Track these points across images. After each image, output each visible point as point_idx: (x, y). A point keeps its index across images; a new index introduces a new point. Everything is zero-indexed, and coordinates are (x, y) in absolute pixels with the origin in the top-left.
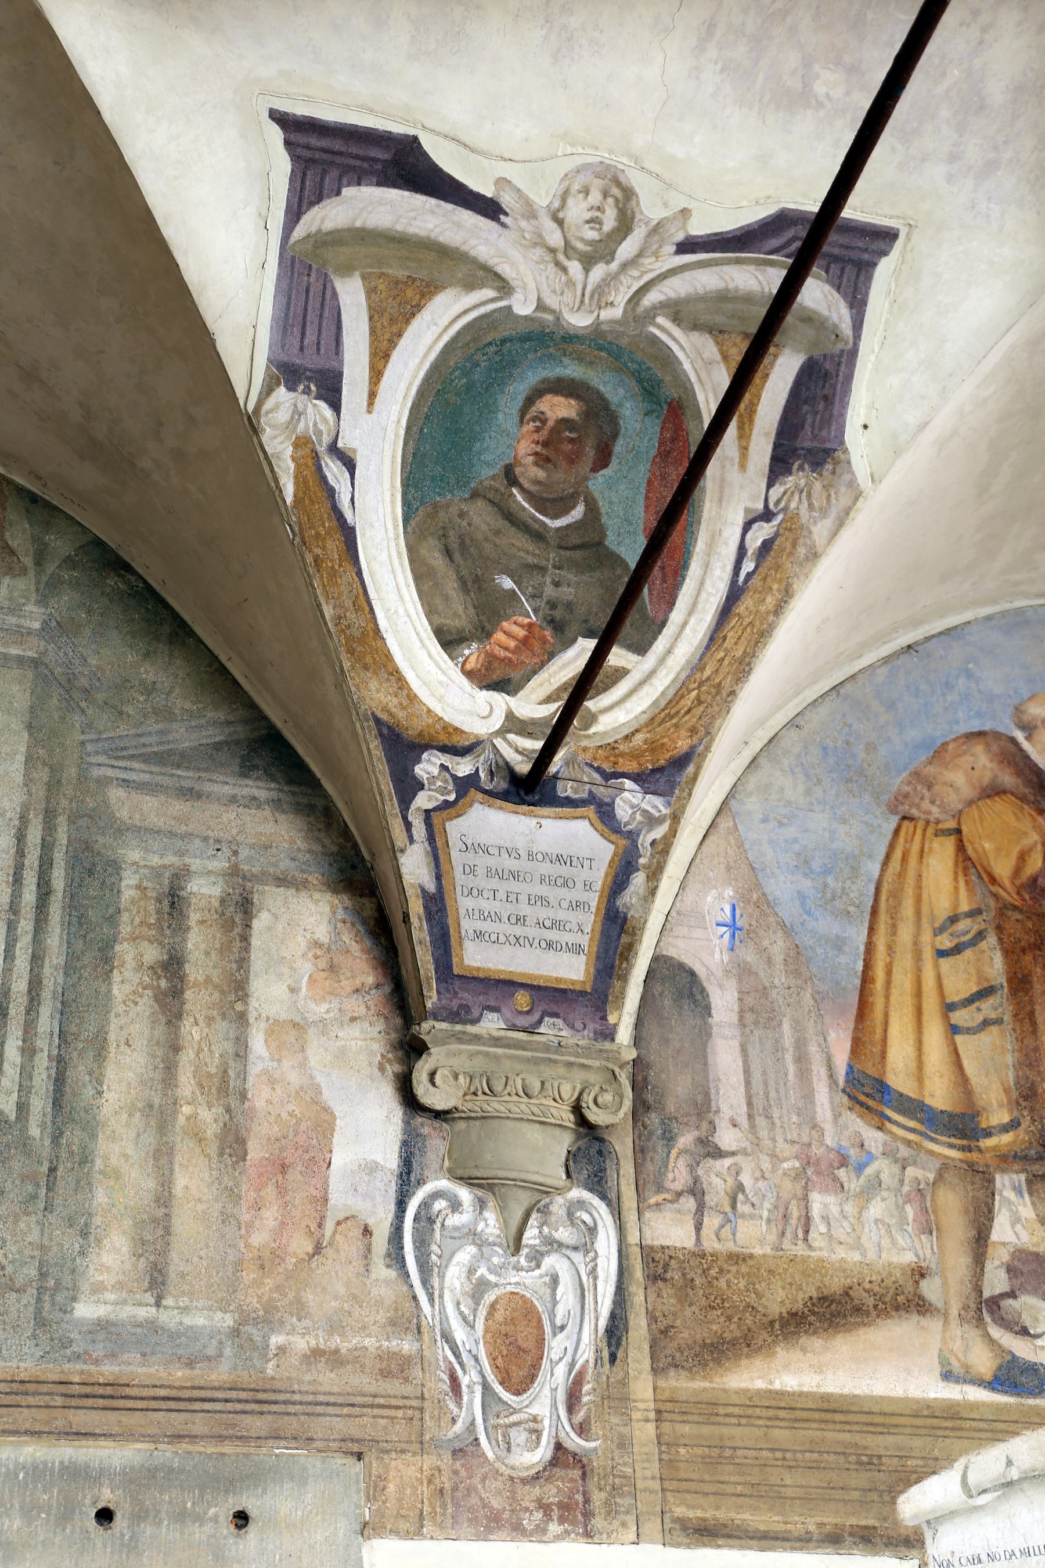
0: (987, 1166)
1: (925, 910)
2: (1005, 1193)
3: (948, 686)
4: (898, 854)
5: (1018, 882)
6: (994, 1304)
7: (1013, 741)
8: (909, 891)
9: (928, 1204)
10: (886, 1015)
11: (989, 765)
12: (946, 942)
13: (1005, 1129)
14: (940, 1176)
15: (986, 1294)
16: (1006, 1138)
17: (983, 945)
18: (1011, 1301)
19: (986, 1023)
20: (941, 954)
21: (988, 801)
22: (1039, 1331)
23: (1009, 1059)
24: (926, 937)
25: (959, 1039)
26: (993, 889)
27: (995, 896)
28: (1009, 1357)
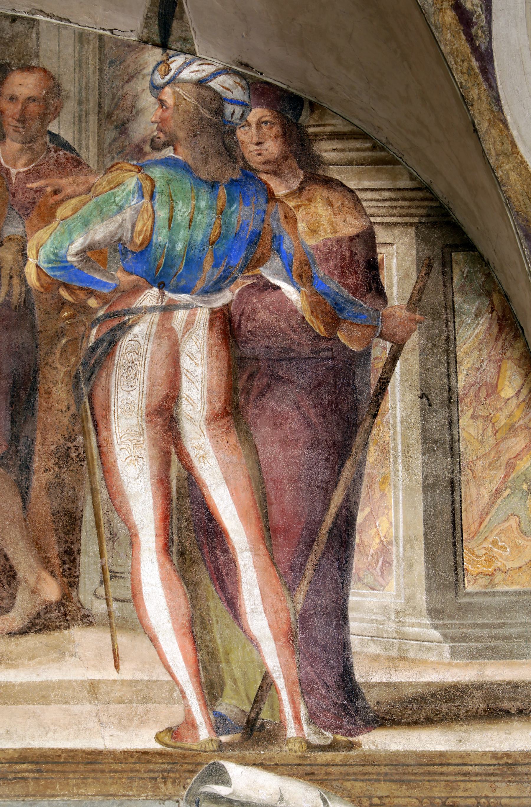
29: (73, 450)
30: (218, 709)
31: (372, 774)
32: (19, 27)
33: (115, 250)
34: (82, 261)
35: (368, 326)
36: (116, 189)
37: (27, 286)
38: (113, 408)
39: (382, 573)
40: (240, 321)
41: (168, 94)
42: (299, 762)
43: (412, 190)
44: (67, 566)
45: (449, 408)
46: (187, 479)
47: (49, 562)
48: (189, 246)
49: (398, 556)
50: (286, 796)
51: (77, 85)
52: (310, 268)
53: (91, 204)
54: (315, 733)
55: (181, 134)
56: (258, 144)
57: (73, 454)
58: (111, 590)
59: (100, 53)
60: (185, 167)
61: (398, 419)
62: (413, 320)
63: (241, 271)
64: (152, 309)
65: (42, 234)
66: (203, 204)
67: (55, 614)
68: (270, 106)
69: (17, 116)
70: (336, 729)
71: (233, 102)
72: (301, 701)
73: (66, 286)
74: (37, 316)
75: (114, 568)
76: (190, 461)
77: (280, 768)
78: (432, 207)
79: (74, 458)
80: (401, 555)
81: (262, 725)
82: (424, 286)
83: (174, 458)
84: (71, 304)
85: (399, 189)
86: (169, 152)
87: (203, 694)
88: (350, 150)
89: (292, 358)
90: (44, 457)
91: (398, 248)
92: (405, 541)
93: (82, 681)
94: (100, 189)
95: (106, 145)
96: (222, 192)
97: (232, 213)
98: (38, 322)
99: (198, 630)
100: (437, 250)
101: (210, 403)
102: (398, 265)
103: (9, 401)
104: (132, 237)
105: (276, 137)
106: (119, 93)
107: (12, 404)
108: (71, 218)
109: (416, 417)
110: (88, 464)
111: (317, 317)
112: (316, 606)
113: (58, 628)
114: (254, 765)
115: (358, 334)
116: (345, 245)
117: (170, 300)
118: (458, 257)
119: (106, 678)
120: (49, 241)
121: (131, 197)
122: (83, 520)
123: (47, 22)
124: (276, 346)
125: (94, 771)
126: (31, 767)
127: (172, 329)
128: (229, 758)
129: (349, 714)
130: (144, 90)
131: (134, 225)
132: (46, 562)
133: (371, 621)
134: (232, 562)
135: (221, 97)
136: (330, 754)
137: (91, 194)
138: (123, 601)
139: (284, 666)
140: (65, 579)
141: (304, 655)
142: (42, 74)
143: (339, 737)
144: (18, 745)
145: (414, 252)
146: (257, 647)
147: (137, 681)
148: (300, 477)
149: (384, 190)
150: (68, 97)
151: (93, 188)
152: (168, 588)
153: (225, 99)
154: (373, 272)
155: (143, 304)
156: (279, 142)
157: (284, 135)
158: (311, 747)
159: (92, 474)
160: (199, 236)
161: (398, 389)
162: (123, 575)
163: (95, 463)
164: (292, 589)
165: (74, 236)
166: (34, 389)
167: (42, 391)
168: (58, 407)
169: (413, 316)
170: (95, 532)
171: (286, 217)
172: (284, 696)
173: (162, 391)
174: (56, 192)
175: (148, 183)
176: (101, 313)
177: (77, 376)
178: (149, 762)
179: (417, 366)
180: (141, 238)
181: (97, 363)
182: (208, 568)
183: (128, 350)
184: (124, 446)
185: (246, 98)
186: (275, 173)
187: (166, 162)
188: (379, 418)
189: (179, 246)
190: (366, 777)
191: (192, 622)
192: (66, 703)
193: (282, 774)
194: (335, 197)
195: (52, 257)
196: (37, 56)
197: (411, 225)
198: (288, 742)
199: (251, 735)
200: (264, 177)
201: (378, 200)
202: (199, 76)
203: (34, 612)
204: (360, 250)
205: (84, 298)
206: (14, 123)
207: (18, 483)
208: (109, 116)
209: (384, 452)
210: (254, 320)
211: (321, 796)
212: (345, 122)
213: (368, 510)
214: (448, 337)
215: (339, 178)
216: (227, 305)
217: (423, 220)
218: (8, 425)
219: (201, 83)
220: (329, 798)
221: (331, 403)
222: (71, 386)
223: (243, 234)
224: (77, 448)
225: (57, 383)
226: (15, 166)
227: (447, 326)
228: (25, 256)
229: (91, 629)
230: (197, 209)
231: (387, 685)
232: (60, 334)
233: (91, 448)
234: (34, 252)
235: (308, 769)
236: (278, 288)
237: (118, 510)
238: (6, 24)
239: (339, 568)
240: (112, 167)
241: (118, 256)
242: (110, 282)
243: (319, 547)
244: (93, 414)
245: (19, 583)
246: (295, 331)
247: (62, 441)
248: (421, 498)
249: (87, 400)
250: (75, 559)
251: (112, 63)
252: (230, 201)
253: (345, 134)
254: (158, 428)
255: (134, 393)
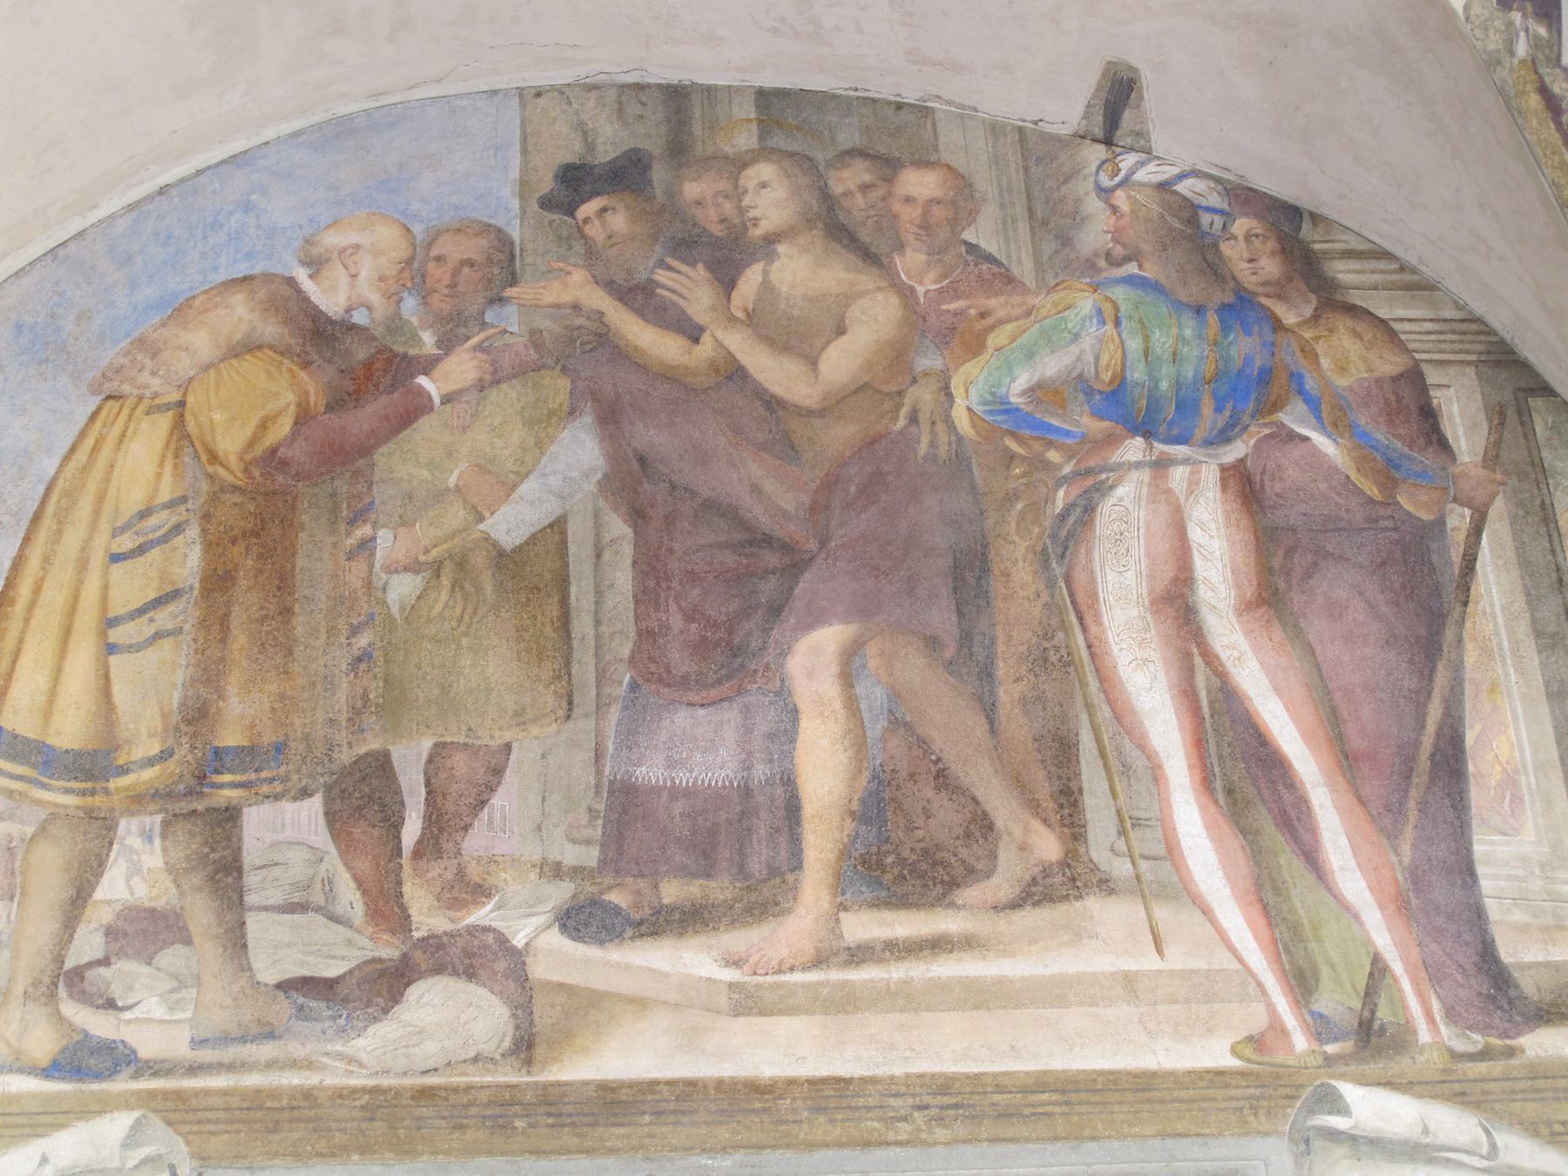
0: (112, 810)
1: (108, 507)
2: (128, 841)
3: (215, 225)
4: (89, 442)
5: (248, 457)
6: (78, 973)
7: (291, 282)
8: (92, 487)
9: (17, 864)
10: (21, 641)
11: (247, 316)
12: (126, 543)
13: (150, 762)
14: (42, 829)
15: (69, 964)
16: (148, 774)
17: (179, 540)
18: (101, 970)
19: (158, 635)
20: (116, 558)
21: (234, 362)
22: (130, 1001)
23: (180, 676)
24: (101, 540)
25: (114, 660)
26: (210, 469)
27: (212, 478)
28: (78, 1037)
29: (1052, 652)
30: (1316, 1007)
31: (1547, 1090)
32: (905, 115)
33: (1075, 389)
34: (1031, 402)
35: (1436, 489)
36: (1067, 313)
37: (957, 434)
38: (1101, 595)
39: (1513, 812)
40: (1262, 480)
41: (1120, 199)
42: (1443, 1078)
43: (1463, 321)
44: (1066, 812)
45: (1561, 593)
46: (1221, 689)
47: (1039, 805)
48: (1178, 384)
49: (1529, 787)
50: (1432, 1127)
51: (995, 185)
52: (1345, 414)
53: (1034, 330)
54: (1458, 1036)
55: (1146, 247)
56: (1251, 261)
57: (1053, 658)
58: (1134, 843)
59: (1022, 148)
60: (1156, 287)
61: (1498, 608)
62: (1493, 481)
63: (1253, 417)
64: (1138, 465)
65: (971, 368)
66: (1188, 333)
67: (1058, 879)
68: (1257, 215)
69: (917, 221)
70: (1486, 1029)
71: (1208, 209)
72: (1432, 992)
73: (1014, 435)
74: (976, 473)
75: (1135, 813)
76: (1222, 664)
77: (1417, 1088)
78: (1491, 343)
79: (1056, 662)
80: (1534, 787)
81: (1382, 1028)
82: (1500, 438)
83: (1198, 661)
84: (1024, 459)
85: (1445, 320)
86: (1132, 268)
87: (1291, 988)
88: (1372, 272)
89: (1342, 529)
90: (1011, 662)
91: (1456, 391)
92: (1536, 769)
93: (1112, 973)
94: (1043, 312)
95: (1045, 259)
96: (1212, 319)
97: (1230, 344)
98: (979, 481)
99: (1269, 897)
100: (1508, 395)
101: (1238, 587)
102: (1460, 411)
103: (951, 586)
104: (1097, 372)
105: (1273, 254)
106: (1055, 196)
107: (955, 590)
108: (1008, 348)
109: (1520, 604)
110: (1076, 670)
111: (1366, 476)
112: (1429, 860)
113: (1066, 898)
114: (1379, 1084)
115: (1423, 498)
116: (1387, 387)
117: (1162, 453)
118: (1536, 403)
119: (1146, 968)
120: (981, 378)
121: (1088, 323)
122: (1081, 747)
123: (944, 110)
124: (1317, 512)
125: (1149, 1101)
126: (1054, 1097)
127: (1169, 491)
128: (1342, 1077)
129: (1500, 1008)
130: (1087, 193)
131: (1097, 359)
132: (1034, 806)
133: (1509, 878)
134: (1302, 801)
135: (1193, 205)
136: (1483, 1064)
137: (1032, 318)
138: (1155, 859)
139: (1399, 944)
140: (1066, 830)
141: (1424, 927)
142: (946, 171)
143: (1492, 1040)
144: (1032, 1066)
145: (1479, 397)
146: (1356, 917)
147: (1192, 971)
148: (1378, 684)
149: (1425, 320)
150: (985, 200)
151: (1034, 312)
152: (1217, 841)
153: (1199, 206)
154: (1431, 421)
155: (1125, 458)
156: (1278, 259)
157: (1283, 251)
158: (1456, 1056)
159: (1084, 684)
160: (1189, 372)
161: (1489, 569)
162: (1149, 823)
163: (1087, 669)
164: (1393, 836)
165: (1016, 371)
166: (985, 570)
167: (997, 572)
168: (1022, 593)
169: (1493, 476)
170: (1101, 763)
171: (1302, 351)
172: (1406, 986)
173: (1167, 573)
174: (983, 316)
175: (1109, 305)
176: (1067, 470)
177: (1044, 551)
178: (1227, 1086)
179: (1510, 539)
180: (1110, 374)
181: (1070, 535)
182: (1270, 811)
183: (1113, 517)
184: (1124, 646)
185: (1225, 206)
186: (1280, 297)
187: (1130, 280)
188: (1470, 604)
189: (1164, 385)
190: (1539, 1095)
191: (1258, 885)
192: (1092, 1005)
193: (1420, 1096)
194: (1361, 327)
195: (988, 397)
196: (936, 149)
197: (1468, 363)
198: (1422, 1049)
199: (1368, 1041)
200: (1265, 301)
201: (1420, 333)
202: (1160, 178)
203: (1028, 877)
204: (1407, 393)
205: (1041, 449)
206: (914, 229)
207: (979, 698)
208: (1045, 223)
209: (1486, 651)
210: (1281, 479)
211: (1481, 1124)
212: (1360, 239)
213: (1478, 728)
214: (1543, 504)
215: (1364, 305)
216: (1242, 460)
217: (1483, 358)
218: (954, 618)
219: (1163, 187)
220: (1493, 1127)
221: (1403, 587)
222: (1037, 566)
223: (1248, 371)
224: (1057, 649)
225: (1017, 561)
226: (921, 283)
227: (1539, 488)
228: (950, 396)
229: (1113, 899)
230: (1181, 338)
231: (1546, 965)
232: (1012, 497)
233: (1078, 649)
234: (962, 390)
235: (1457, 1087)
236: (1307, 439)
237: (1129, 733)
238: (890, 112)
239: (1452, 806)
240: (1056, 285)
241: (1081, 396)
242: (1074, 430)
243: (1420, 779)
244: (1074, 603)
245: (999, 837)
246: (1339, 494)
247: (1035, 640)
248: (1547, 710)
249: (1062, 584)
250: (1076, 801)
251: (1039, 160)
252: (1225, 329)
253: (1362, 252)
254: (1169, 621)
255: (1128, 574)
